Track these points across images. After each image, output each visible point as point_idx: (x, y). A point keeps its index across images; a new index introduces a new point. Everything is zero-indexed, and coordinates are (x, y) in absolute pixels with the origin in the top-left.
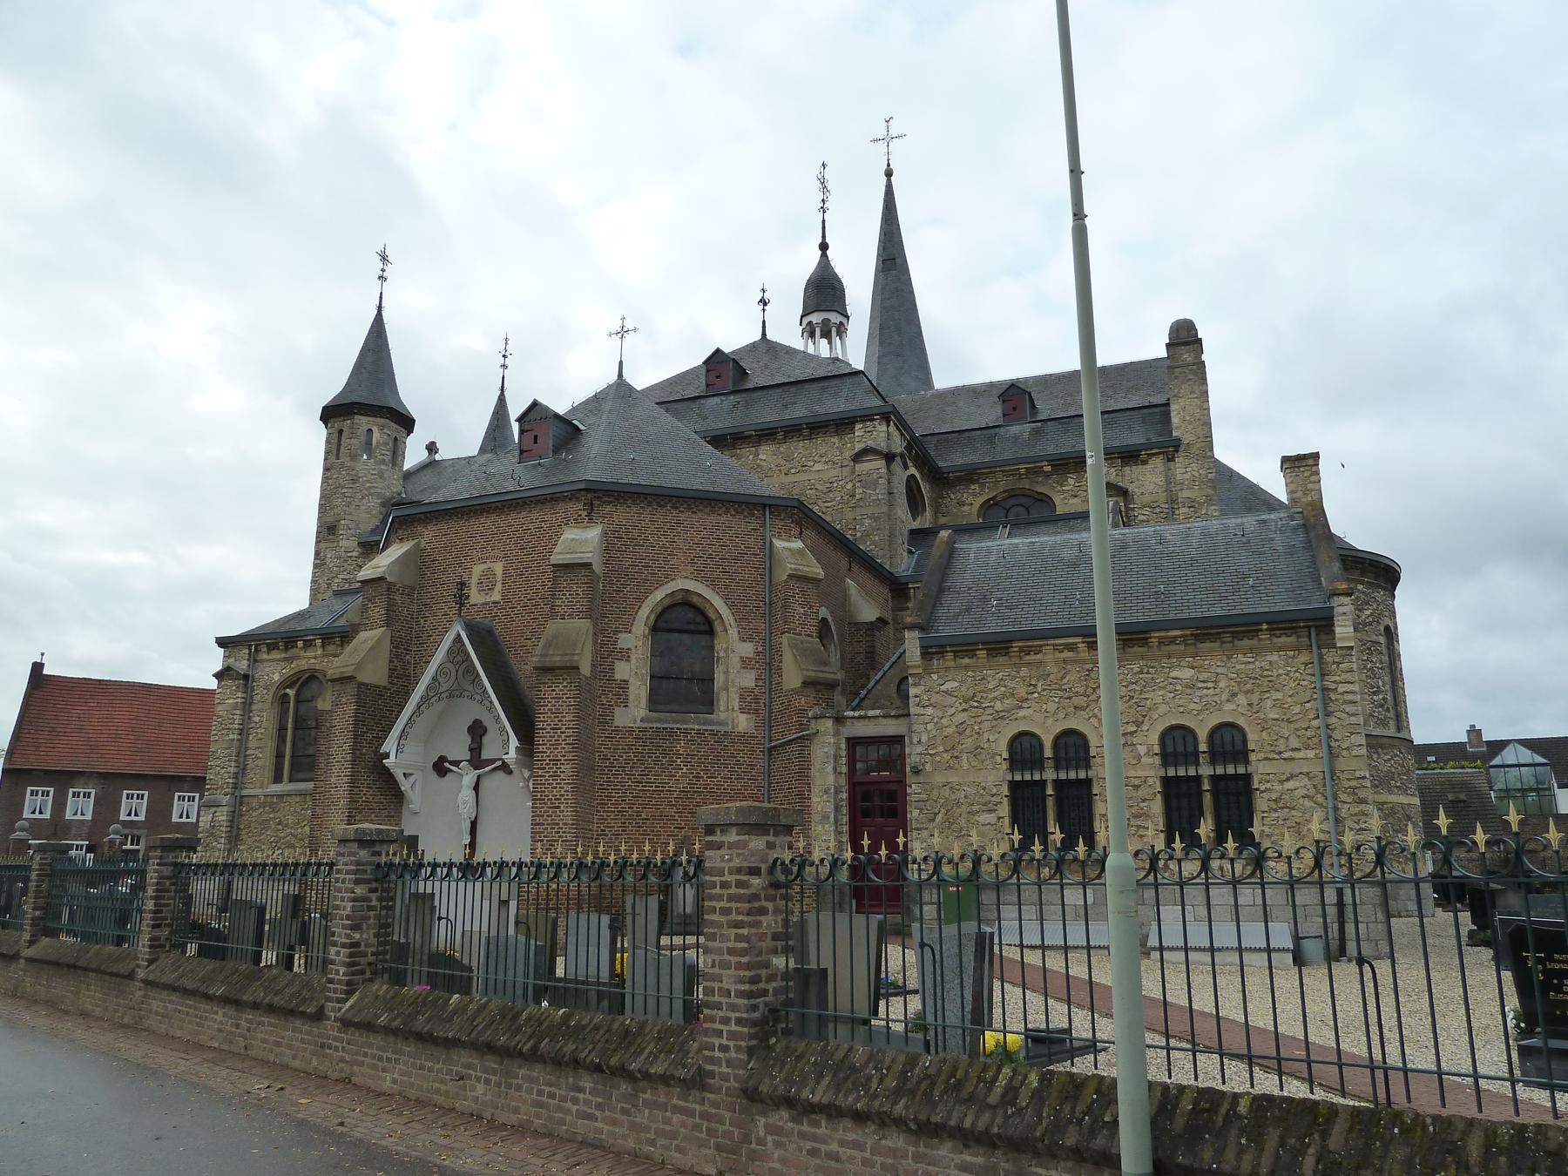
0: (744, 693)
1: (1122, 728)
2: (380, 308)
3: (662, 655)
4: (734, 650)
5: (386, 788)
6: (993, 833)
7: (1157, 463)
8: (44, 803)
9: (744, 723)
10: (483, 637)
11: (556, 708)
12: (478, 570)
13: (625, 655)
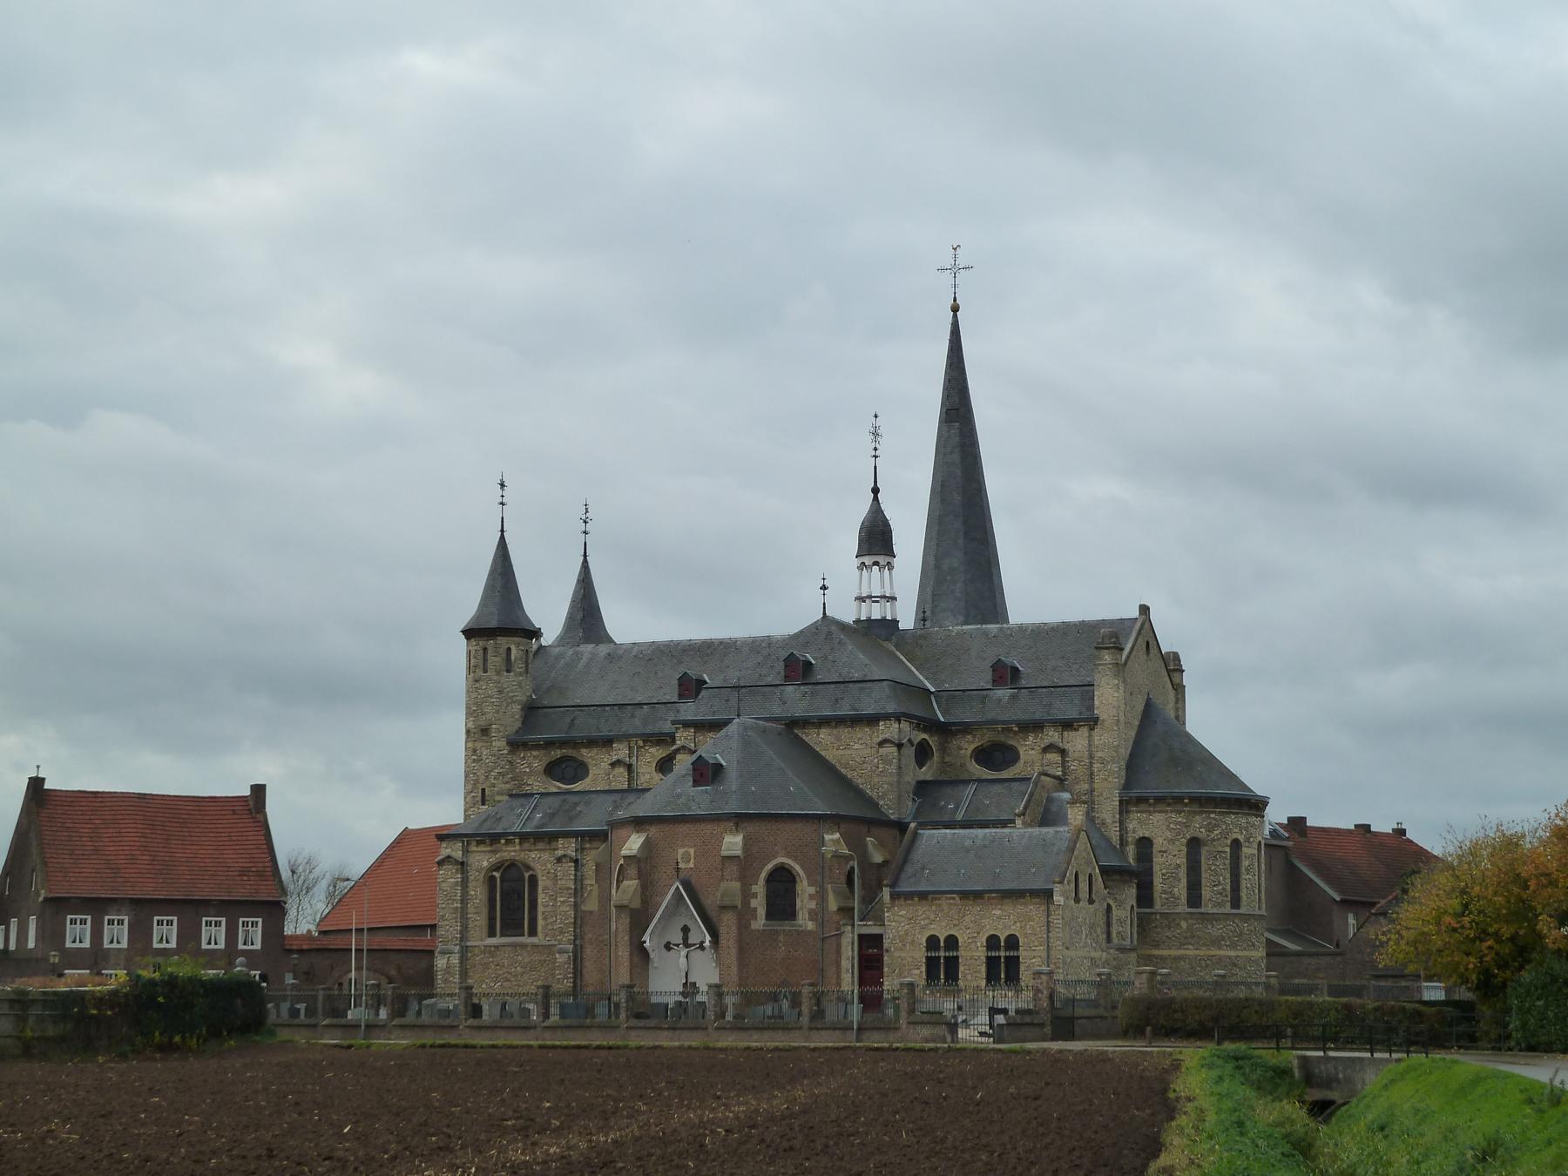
0: (811, 912)
1: (971, 932)
2: (502, 538)
3: (691, 687)
4: (805, 892)
5: (641, 955)
6: (918, 975)
7: (1084, 731)
8: (83, 932)
9: (810, 926)
10: (687, 885)
11: (728, 925)
12: (681, 851)
13: (755, 895)
